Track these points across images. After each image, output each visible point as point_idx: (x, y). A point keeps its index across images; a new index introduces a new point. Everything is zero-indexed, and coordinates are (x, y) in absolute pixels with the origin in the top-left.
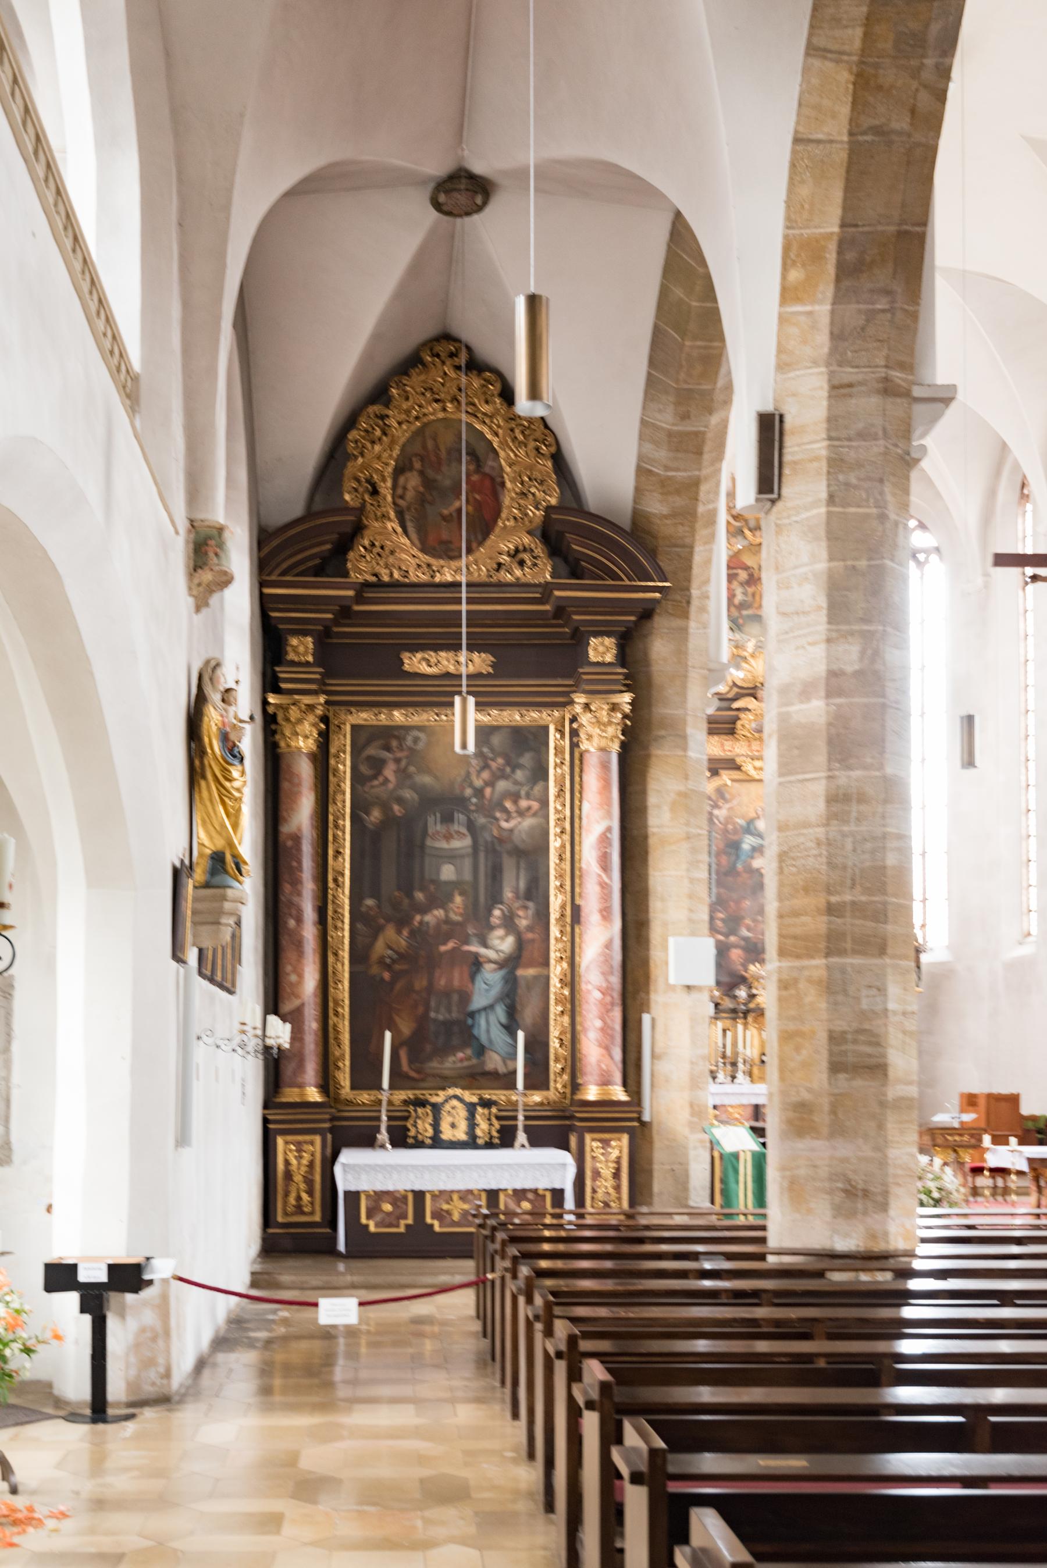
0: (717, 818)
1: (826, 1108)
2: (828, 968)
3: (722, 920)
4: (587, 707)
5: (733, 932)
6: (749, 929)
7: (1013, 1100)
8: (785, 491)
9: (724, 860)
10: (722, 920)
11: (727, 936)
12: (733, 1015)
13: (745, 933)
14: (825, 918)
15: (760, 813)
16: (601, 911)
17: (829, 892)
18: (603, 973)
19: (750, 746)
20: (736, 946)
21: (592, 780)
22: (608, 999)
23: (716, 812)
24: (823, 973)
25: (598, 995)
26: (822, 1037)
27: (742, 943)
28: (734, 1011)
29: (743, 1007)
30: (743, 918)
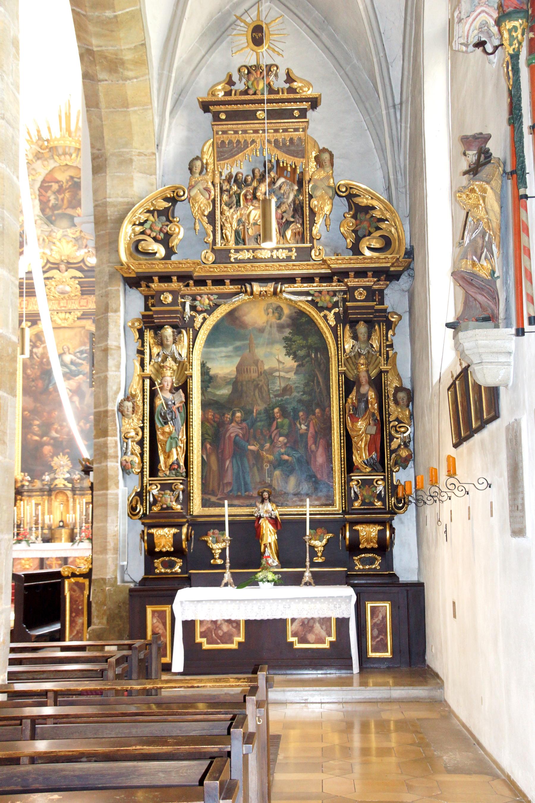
0: (36, 354)
3: (38, 426)
5: (45, 433)
6: (57, 432)
9: (40, 383)
10: (38, 426)
11: (42, 437)
12: (41, 493)
13: (54, 434)
15: (66, 350)
19: (59, 304)
20: (48, 444)
23: (35, 350)
27: (52, 441)
28: (42, 490)
29: (47, 487)
30: (53, 424)
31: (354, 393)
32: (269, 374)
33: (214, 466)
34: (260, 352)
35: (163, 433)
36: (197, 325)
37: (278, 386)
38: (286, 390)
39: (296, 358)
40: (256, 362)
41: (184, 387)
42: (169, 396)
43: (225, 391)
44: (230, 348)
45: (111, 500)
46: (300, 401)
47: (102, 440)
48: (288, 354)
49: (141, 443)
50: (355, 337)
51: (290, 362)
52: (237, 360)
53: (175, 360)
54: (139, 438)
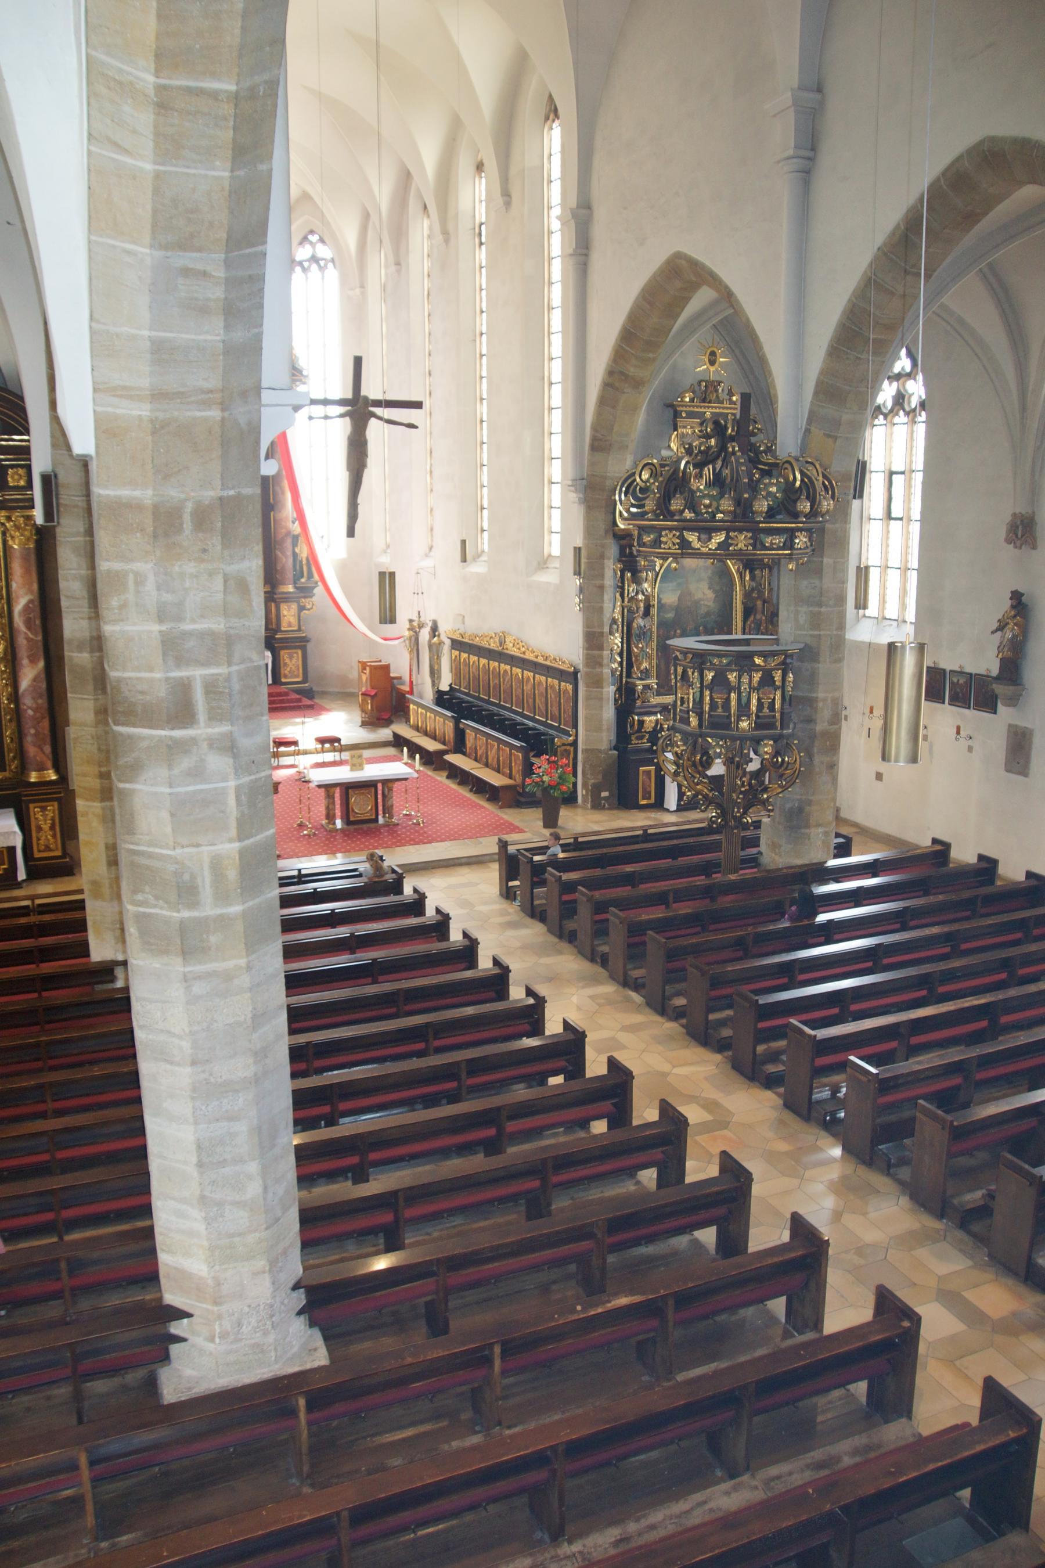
1: (107, 885)
2: (103, 809)
4: (9, 519)
7: (386, 668)
8: (62, 521)
14: (98, 781)
16: (28, 657)
17: (100, 766)
18: (33, 698)
21: (17, 568)
22: (38, 715)
24: (99, 811)
25: (30, 712)
26: (102, 847)
31: (752, 618)
32: (697, 603)
33: (663, 666)
34: (693, 587)
35: (637, 647)
36: (657, 569)
37: (703, 611)
38: (708, 614)
39: (715, 591)
40: (690, 594)
41: (647, 613)
42: (640, 622)
43: (670, 615)
44: (675, 584)
45: (605, 696)
46: (716, 622)
47: (596, 652)
48: (710, 588)
49: (621, 655)
50: (753, 578)
51: (710, 594)
52: (679, 592)
53: (643, 594)
54: (619, 650)
